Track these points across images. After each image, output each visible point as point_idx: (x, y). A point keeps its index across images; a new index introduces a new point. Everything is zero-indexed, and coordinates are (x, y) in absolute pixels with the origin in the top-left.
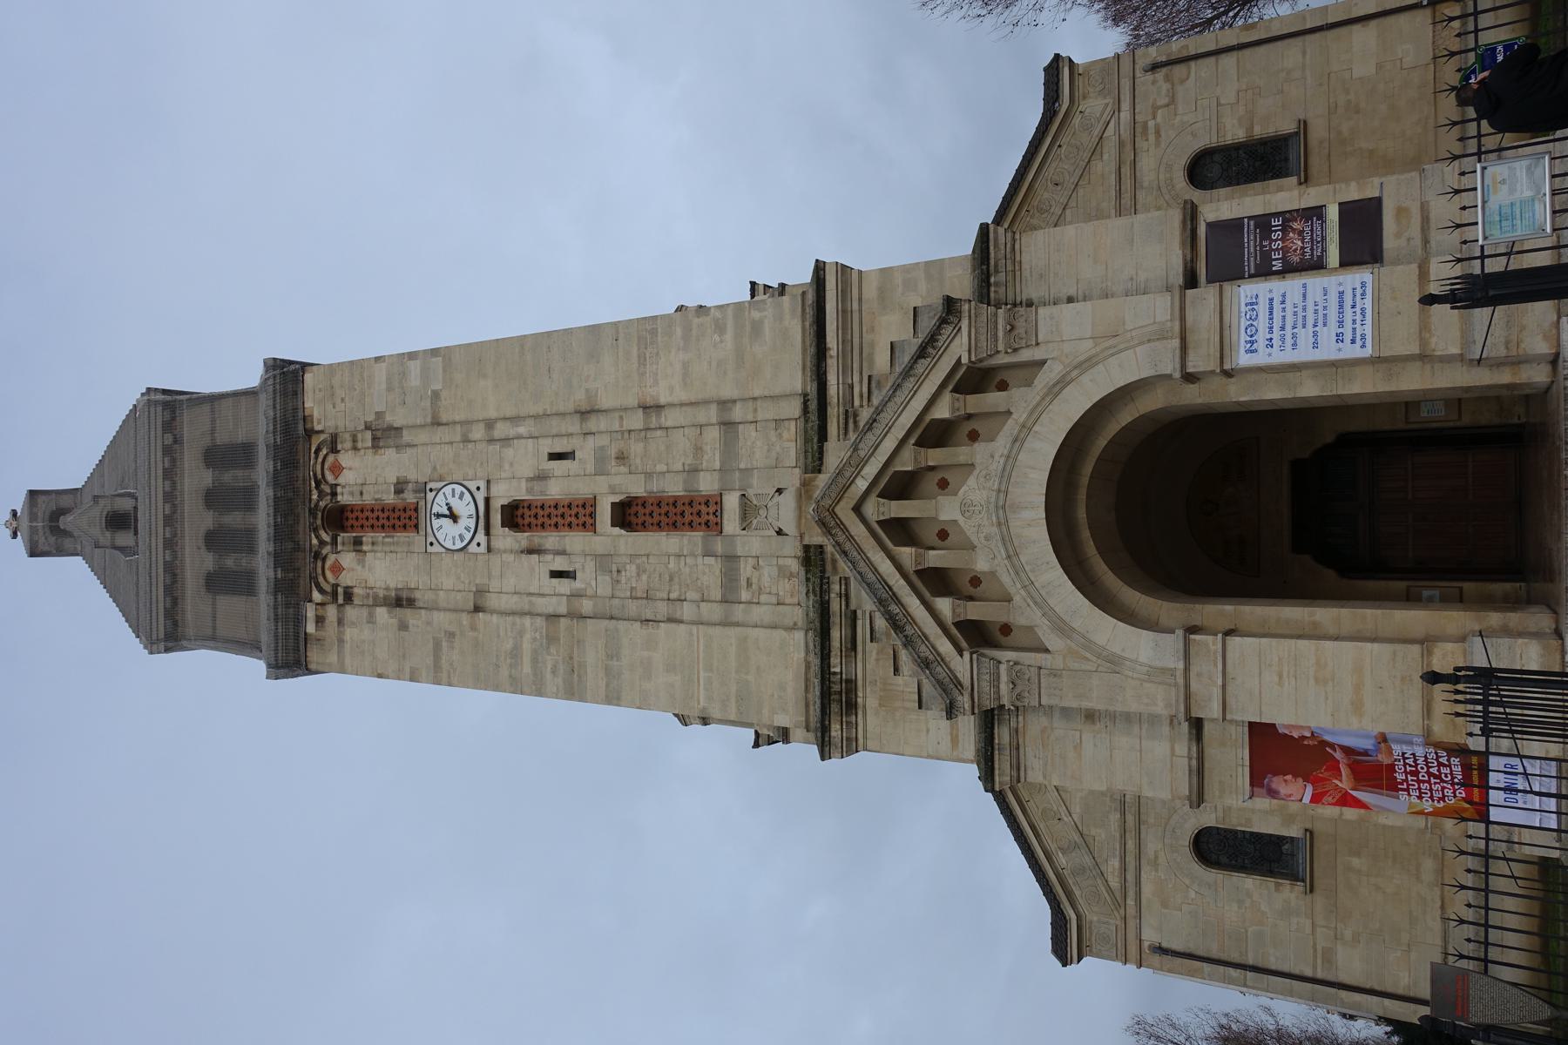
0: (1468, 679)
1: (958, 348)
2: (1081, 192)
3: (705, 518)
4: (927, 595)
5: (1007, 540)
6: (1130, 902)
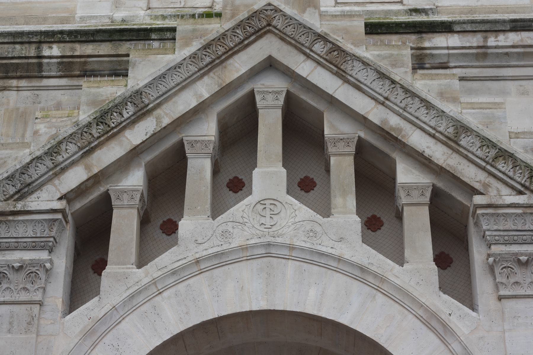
4: (148, 157)
5: (221, 259)
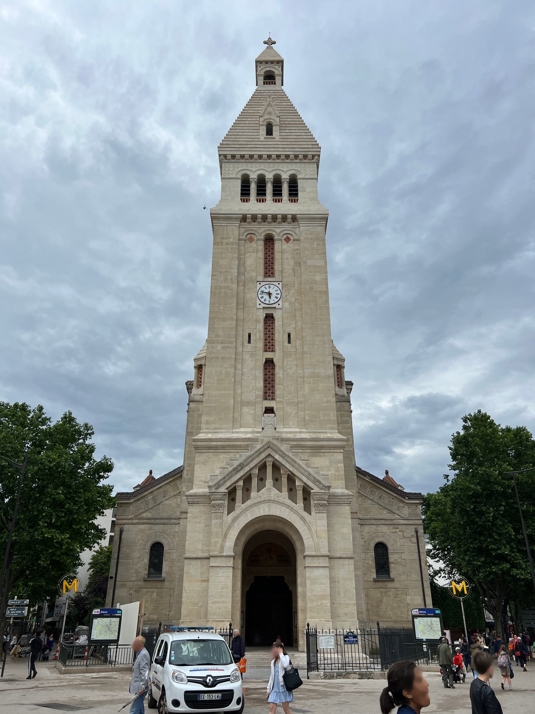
0: (230, 631)
1: (315, 489)
2: (377, 506)
3: (268, 392)
4: (244, 478)
5: (259, 503)
6: (136, 521)
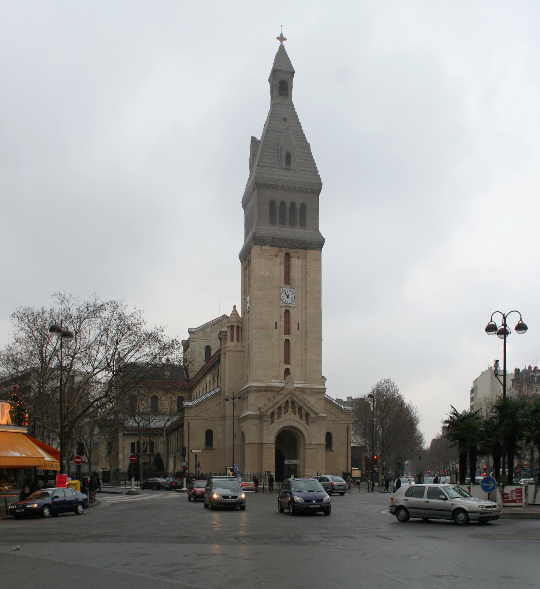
1: (312, 415)
